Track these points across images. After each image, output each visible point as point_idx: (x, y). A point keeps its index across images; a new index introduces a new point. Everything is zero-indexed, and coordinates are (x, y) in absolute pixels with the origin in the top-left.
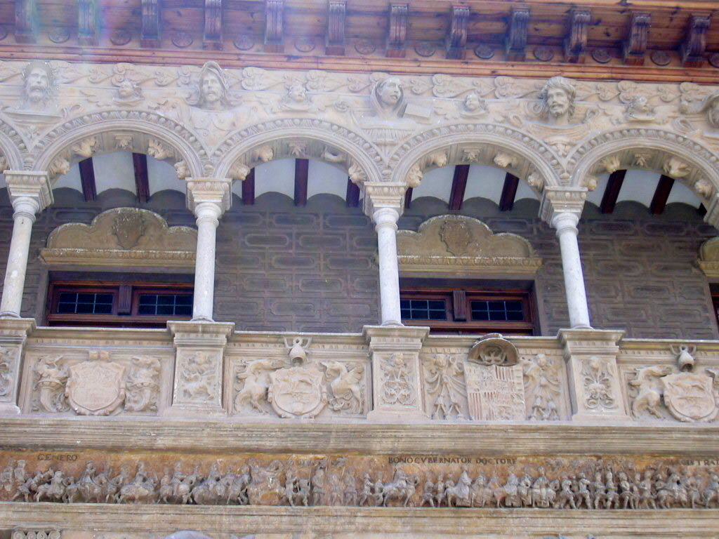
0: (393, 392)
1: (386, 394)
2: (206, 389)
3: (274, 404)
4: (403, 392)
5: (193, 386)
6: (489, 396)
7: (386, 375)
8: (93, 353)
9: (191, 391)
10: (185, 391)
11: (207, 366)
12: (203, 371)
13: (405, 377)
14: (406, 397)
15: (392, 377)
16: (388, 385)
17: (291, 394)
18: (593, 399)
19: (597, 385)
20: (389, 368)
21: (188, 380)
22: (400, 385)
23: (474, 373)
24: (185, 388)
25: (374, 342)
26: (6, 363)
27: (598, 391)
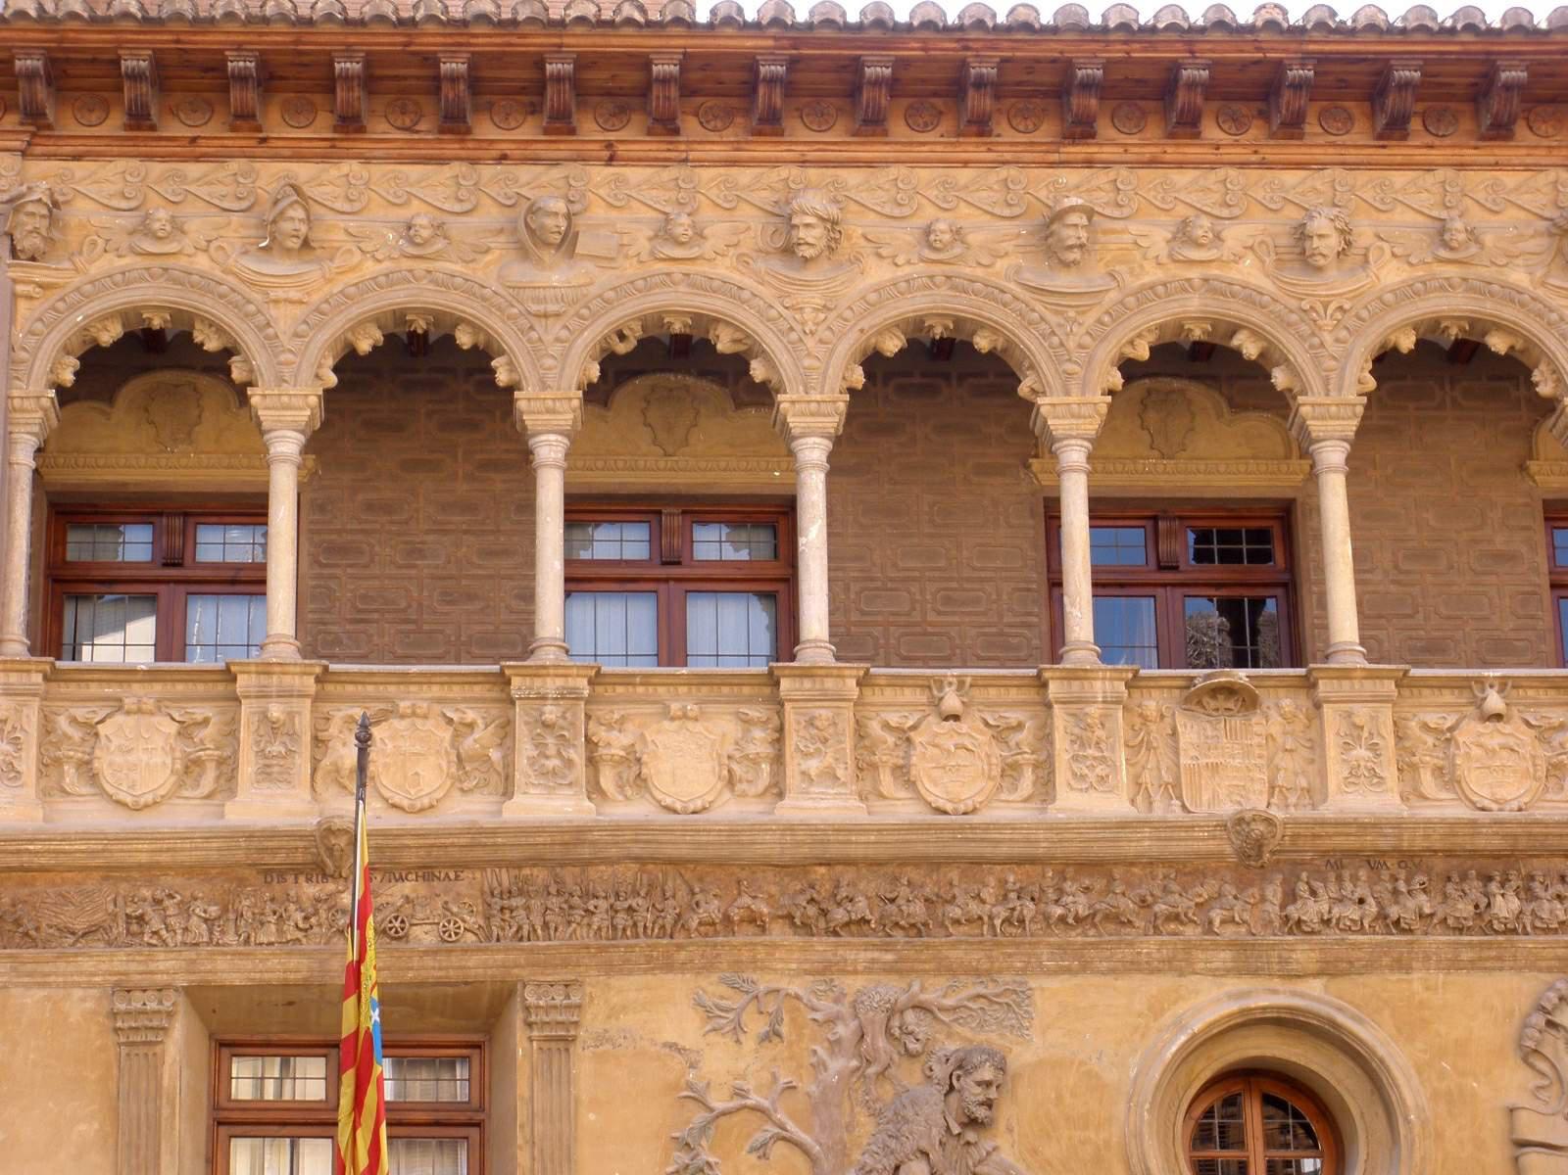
0: (1086, 771)
1: (1074, 774)
2: (834, 769)
3: (919, 784)
4: (1098, 770)
5: (813, 765)
6: (1215, 768)
7: (1073, 742)
8: (675, 707)
9: (813, 773)
10: (803, 773)
11: (831, 730)
12: (826, 740)
13: (1103, 746)
14: (1102, 779)
15: (1083, 746)
16: (1075, 758)
17: (944, 768)
18: (1353, 775)
19: (1361, 753)
20: (1077, 731)
21: (807, 755)
22: (1095, 758)
23: (1191, 731)
24: (803, 767)
25: (1054, 689)
26: (566, 733)
27: (1362, 764)
